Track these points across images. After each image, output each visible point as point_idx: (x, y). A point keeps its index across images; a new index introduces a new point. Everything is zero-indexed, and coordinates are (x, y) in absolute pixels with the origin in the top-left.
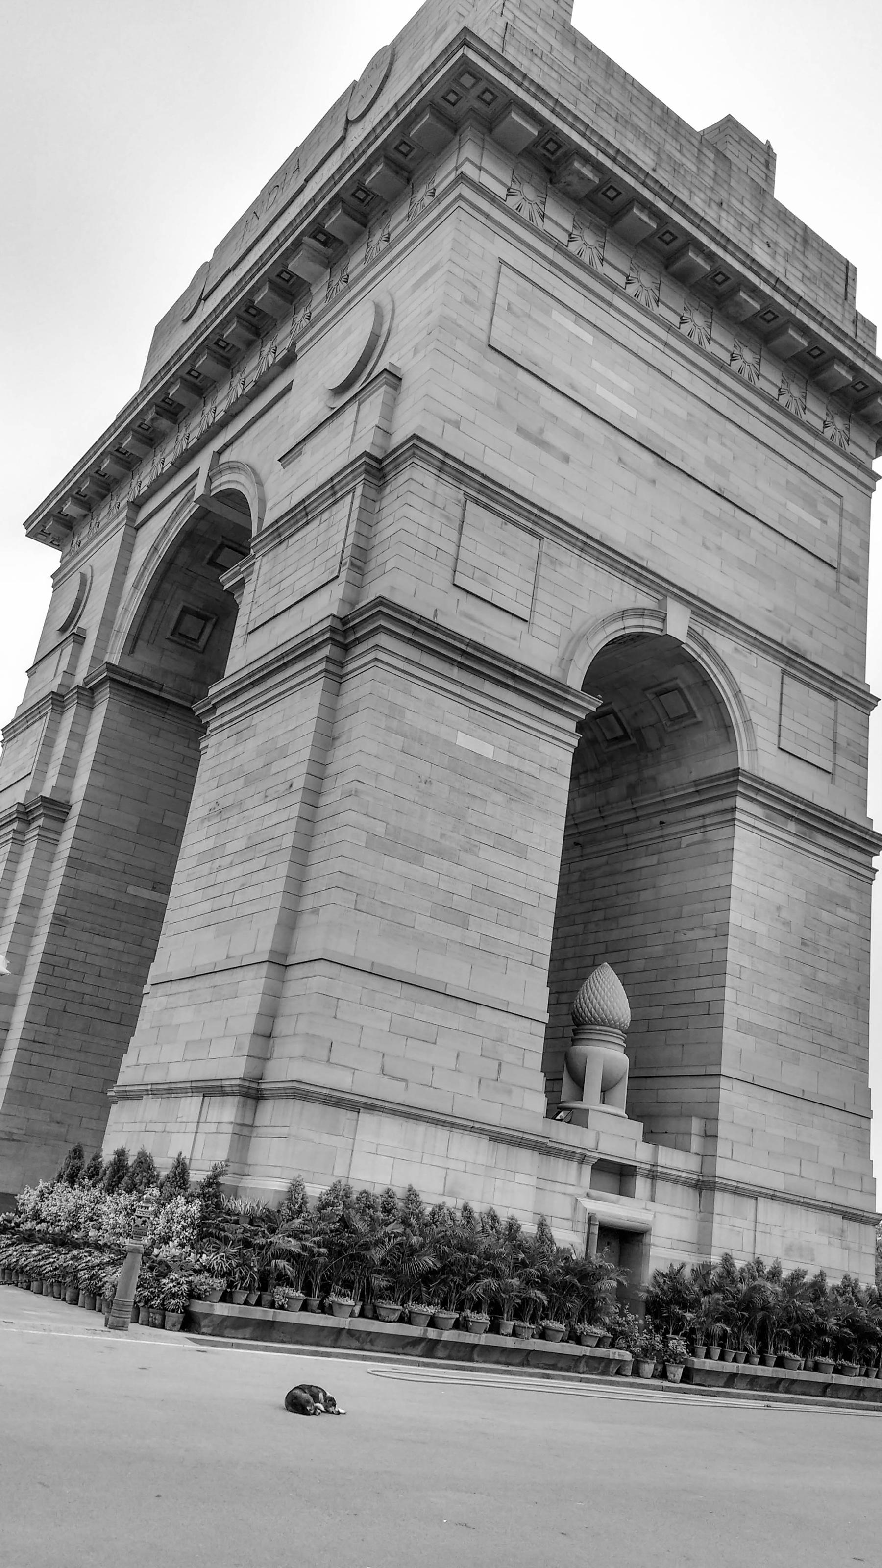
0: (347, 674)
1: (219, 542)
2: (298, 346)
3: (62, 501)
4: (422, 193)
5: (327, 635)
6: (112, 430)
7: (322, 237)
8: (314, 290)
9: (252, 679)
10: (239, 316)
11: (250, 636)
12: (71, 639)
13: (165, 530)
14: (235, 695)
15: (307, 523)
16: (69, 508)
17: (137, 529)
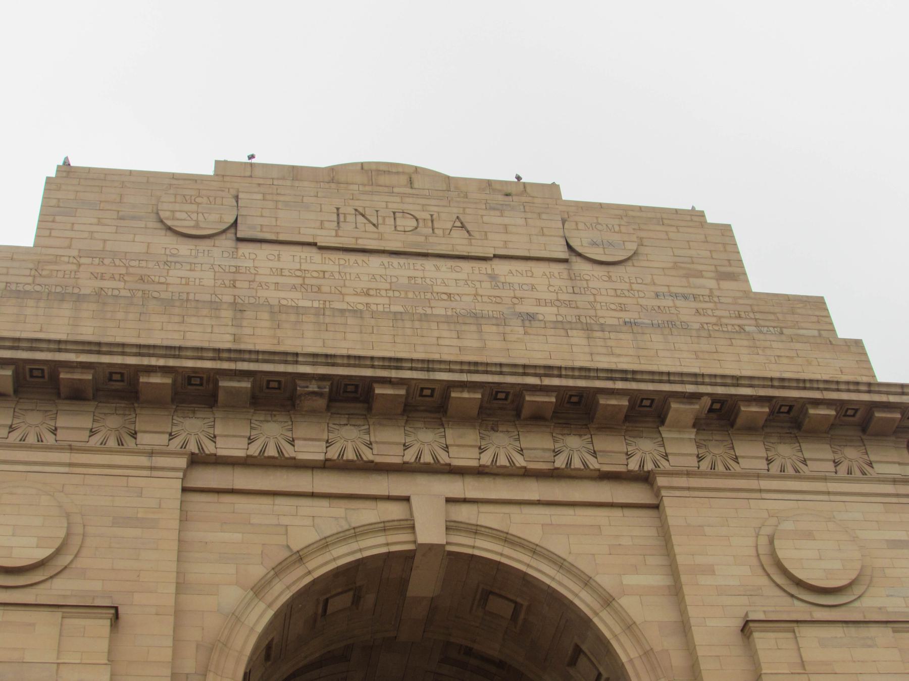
2: (661, 481)
4: (852, 454)
6: (211, 354)
7: (717, 406)
13: (325, 544)
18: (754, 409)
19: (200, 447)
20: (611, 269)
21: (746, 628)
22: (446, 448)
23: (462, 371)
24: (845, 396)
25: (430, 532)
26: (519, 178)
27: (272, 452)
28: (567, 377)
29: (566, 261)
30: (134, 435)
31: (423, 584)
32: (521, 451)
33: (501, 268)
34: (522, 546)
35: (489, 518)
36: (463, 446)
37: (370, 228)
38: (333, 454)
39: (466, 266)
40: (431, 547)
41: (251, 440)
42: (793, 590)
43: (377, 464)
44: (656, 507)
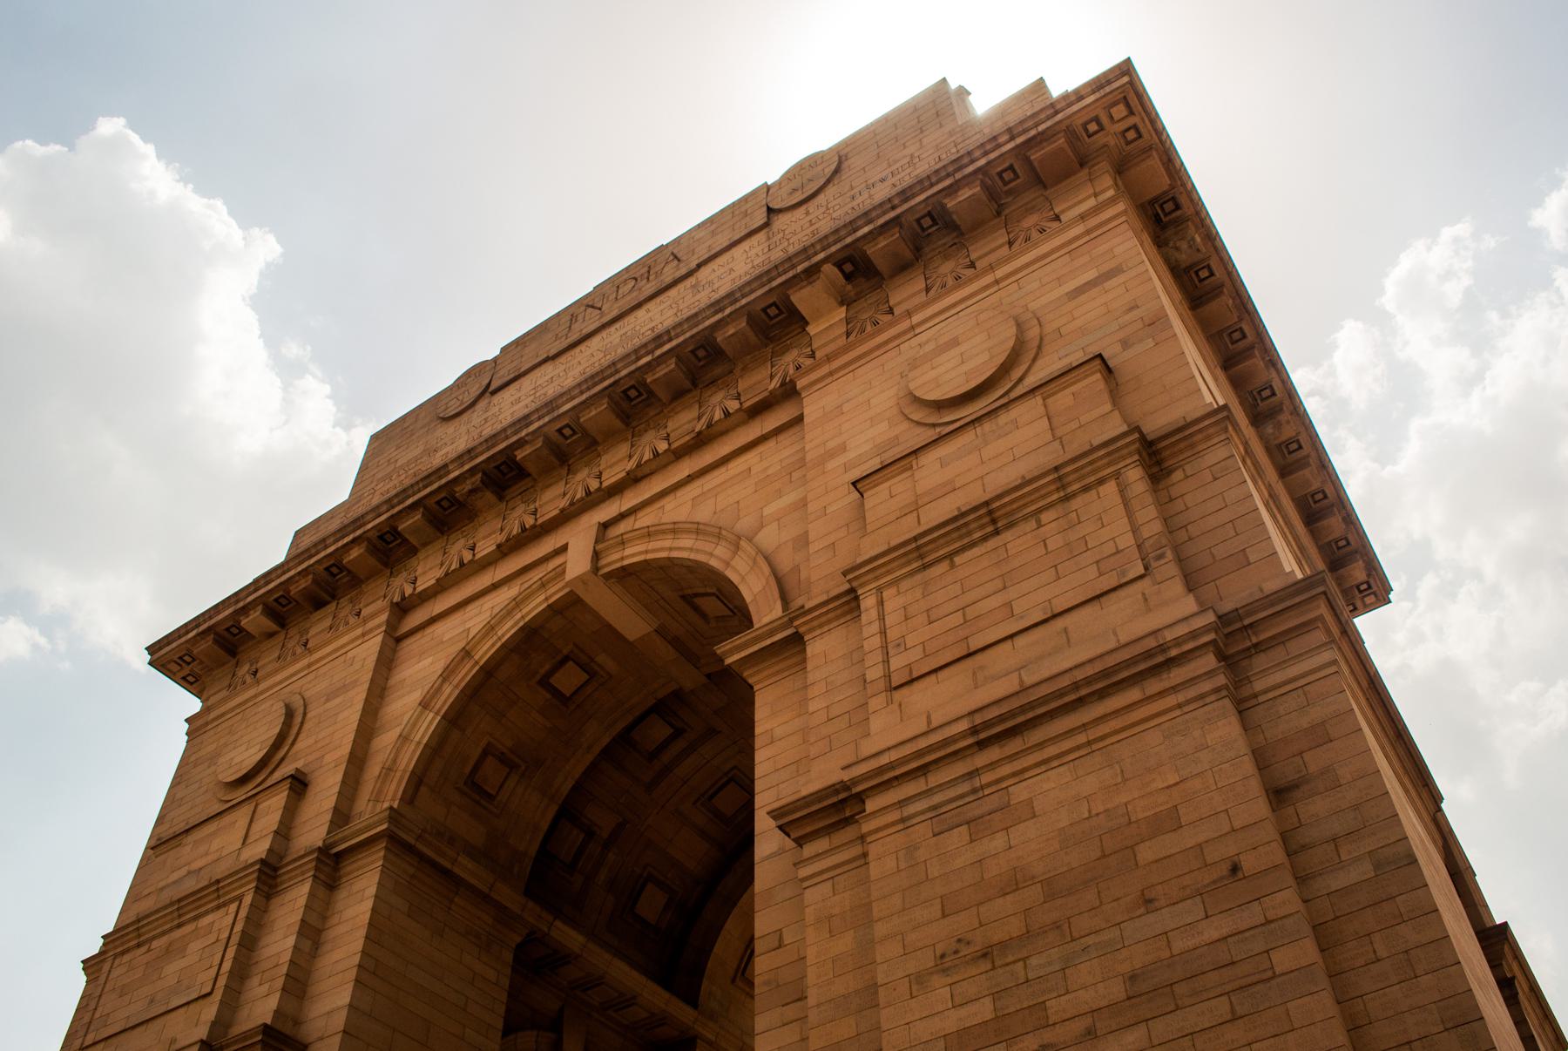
0: (1255, 696)
1: (565, 652)
3: (245, 610)
5: (1212, 636)
6: (384, 508)
7: (848, 267)
8: (812, 330)
9: (983, 736)
10: (679, 358)
11: (897, 695)
12: (287, 785)
13: (490, 628)
14: (923, 770)
15: (997, 532)
16: (255, 621)
17: (399, 640)
18: (882, 242)
20: (811, 206)
23: (582, 393)
28: (677, 336)
29: (766, 225)
31: (632, 623)
32: (667, 438)
33: (704, 273)
34: (663, 532)
36: (615, 464)
39: (673, 292)
40: (581, 579)
43: (541, 525)
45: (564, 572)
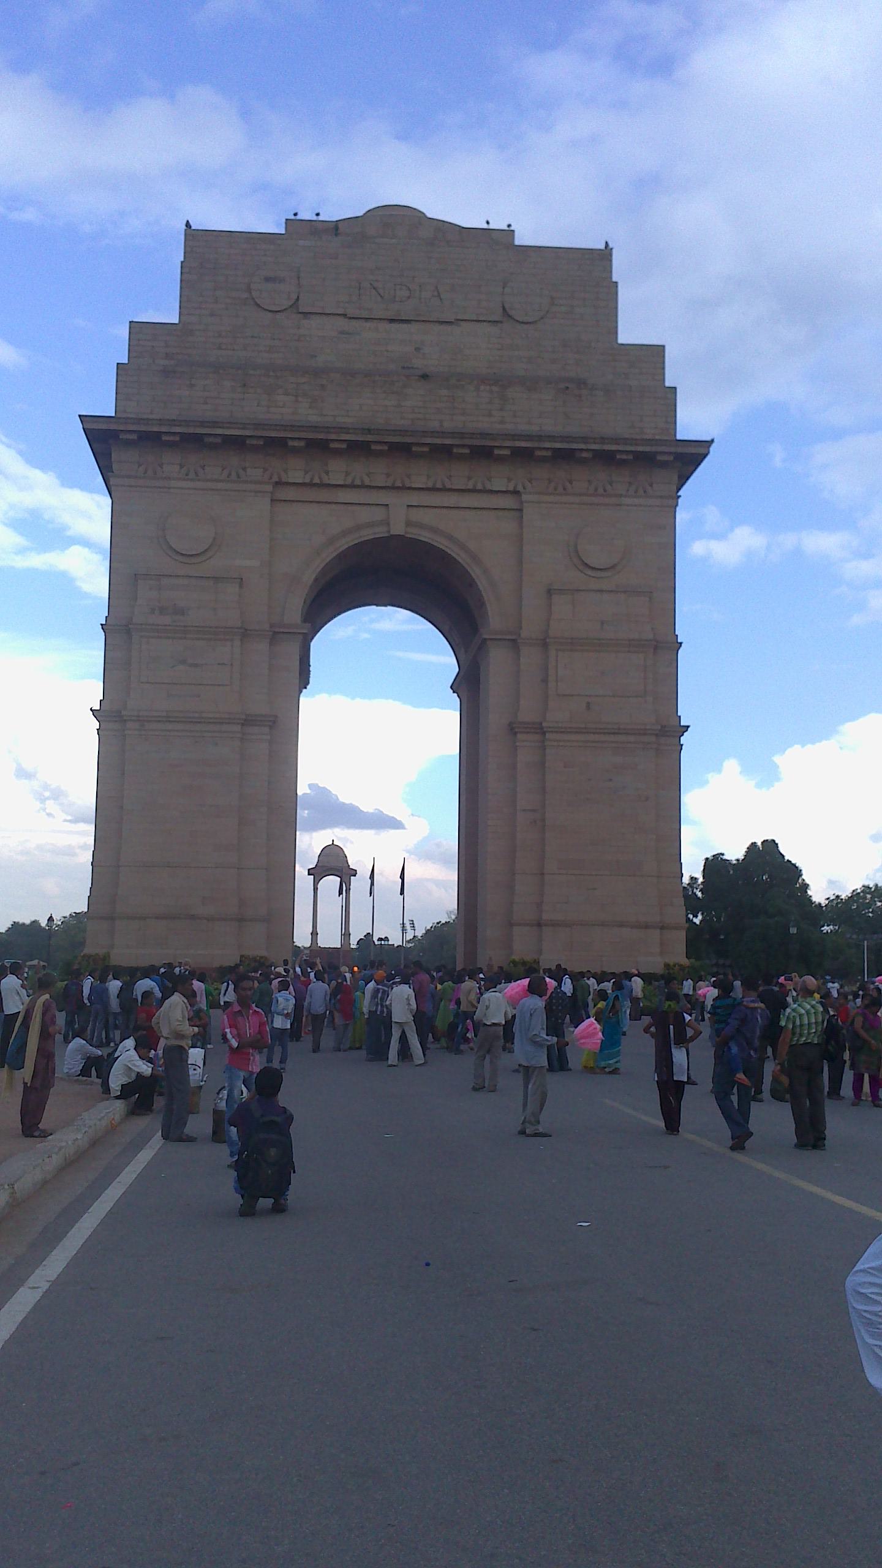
2: (524, 497)
19: (279, 478)
21: (550, 592)
22: (409, 476)
24: (640, 449)
25: (398, 529)
26: (488, 223)
27: (316, 480)
30: (244, 469)
35: (428, 517)
36: (420, 474)
37: (379, 299)
38: (349, 481)
41: (306, 472)
42: (581, 567)
44: (521, 510)
45: (388, 524)
